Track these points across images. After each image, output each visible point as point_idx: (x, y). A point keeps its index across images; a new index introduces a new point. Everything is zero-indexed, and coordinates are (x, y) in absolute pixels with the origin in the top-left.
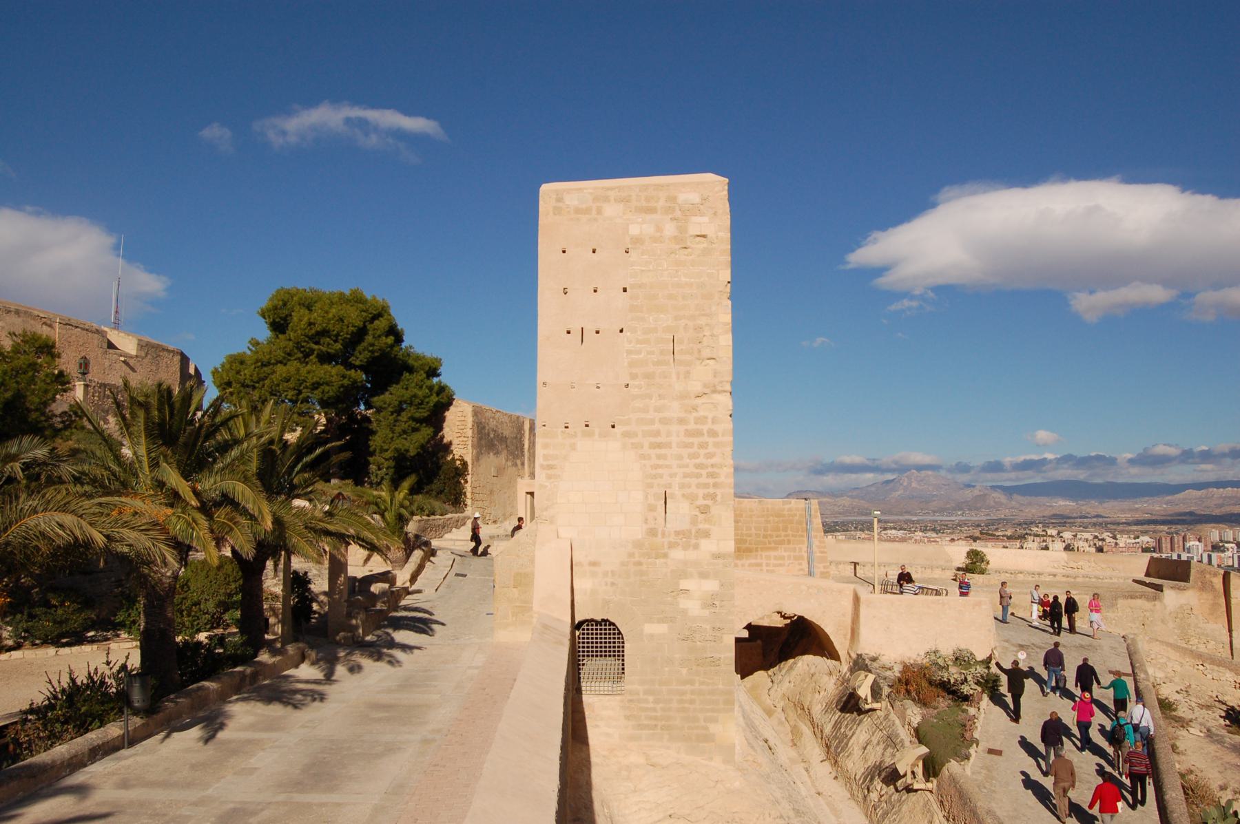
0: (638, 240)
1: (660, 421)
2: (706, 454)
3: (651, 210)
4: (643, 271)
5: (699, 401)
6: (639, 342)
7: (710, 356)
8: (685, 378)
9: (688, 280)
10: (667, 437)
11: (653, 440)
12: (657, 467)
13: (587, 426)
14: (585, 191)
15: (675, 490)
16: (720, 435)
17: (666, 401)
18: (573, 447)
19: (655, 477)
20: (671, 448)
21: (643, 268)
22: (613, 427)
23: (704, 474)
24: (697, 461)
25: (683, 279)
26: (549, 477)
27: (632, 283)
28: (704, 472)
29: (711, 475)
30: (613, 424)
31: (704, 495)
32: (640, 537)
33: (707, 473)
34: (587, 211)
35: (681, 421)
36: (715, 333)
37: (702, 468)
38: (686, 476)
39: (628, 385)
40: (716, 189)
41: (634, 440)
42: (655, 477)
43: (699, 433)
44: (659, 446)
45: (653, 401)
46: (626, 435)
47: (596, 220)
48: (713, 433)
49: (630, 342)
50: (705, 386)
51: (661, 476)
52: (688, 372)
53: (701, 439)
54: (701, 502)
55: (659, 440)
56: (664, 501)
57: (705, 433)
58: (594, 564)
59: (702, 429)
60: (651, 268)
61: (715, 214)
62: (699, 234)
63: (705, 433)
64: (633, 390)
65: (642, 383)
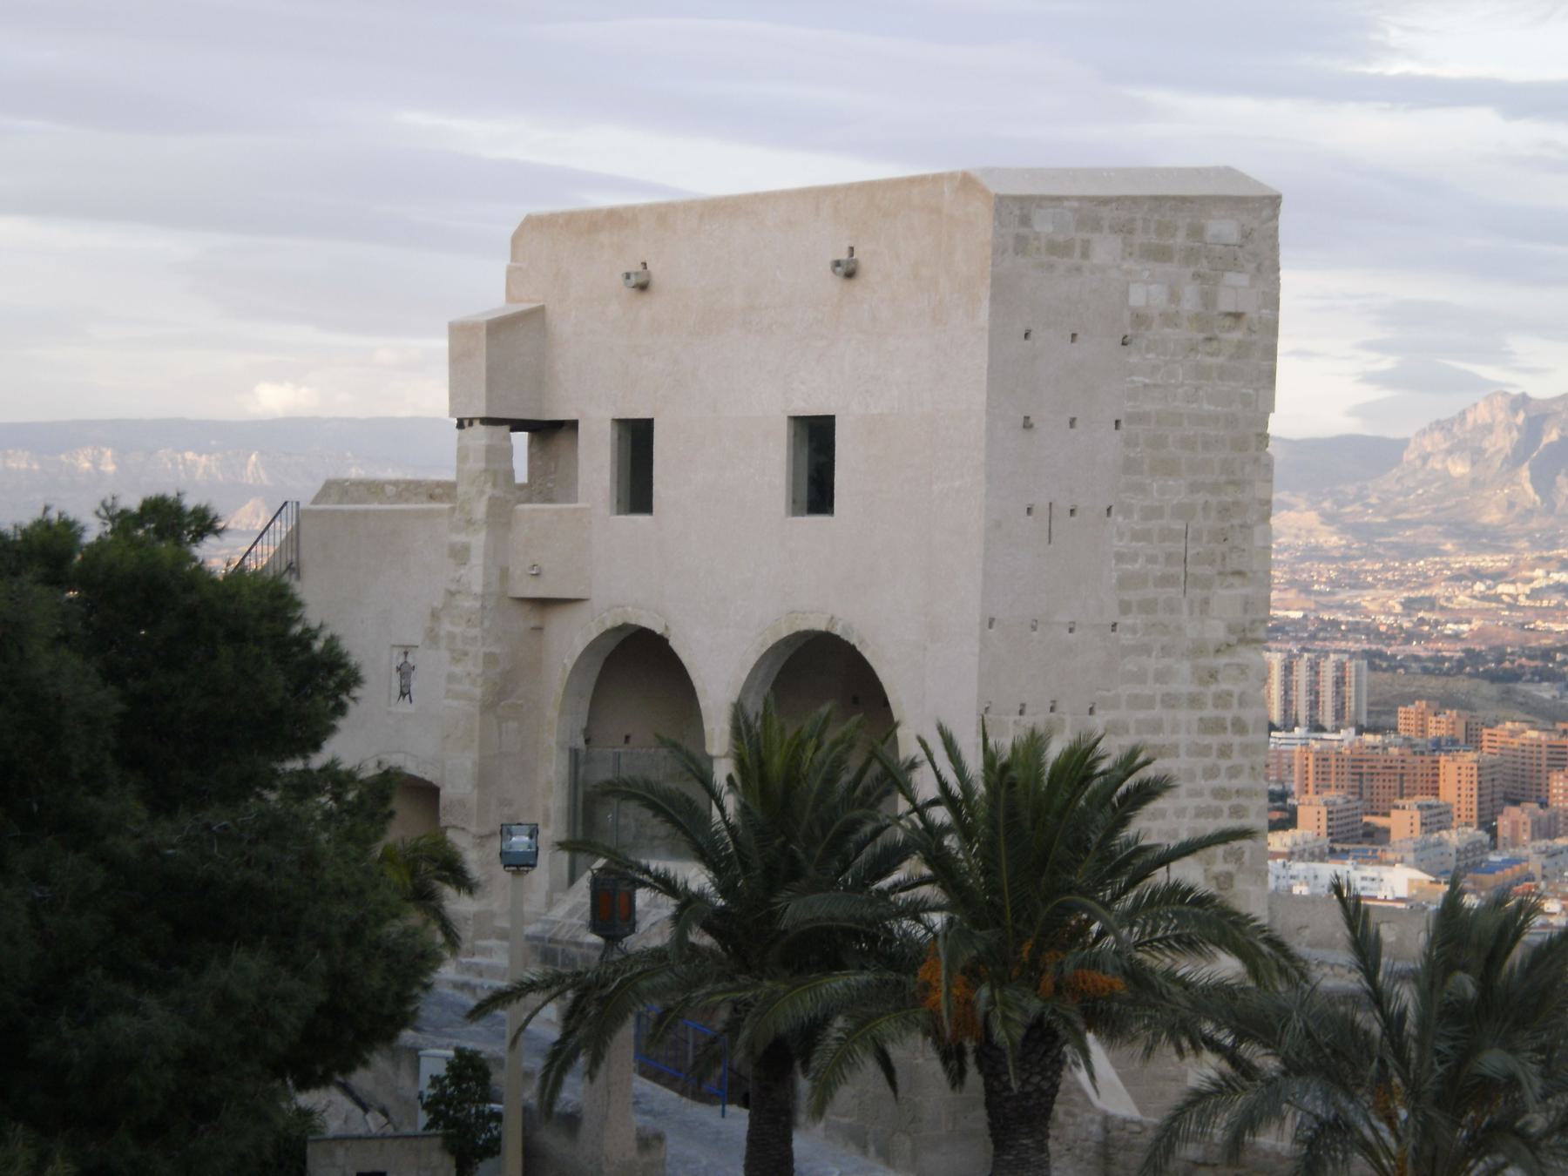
1: (1163, 701)
3: (1161, 254)
4: (1146, 386)
5: (1223, 660)
6: (1136, 536)
9: (1212, 408)
14: (1066, 204)
16: (1251, 730)
20: (1178, 756)
21: (1147, 381)
23: (1226, 812)
27: (1129, 410)
28: (1225, 805)
35: (1195, 701)
36: (1249, 521)
47: (1078, 269)
49: (1121, 536)
50: (1231, 629)
52: (1206, 601)
59: (1224, 719)
61: (1258, 269)
65: (1138, 621)
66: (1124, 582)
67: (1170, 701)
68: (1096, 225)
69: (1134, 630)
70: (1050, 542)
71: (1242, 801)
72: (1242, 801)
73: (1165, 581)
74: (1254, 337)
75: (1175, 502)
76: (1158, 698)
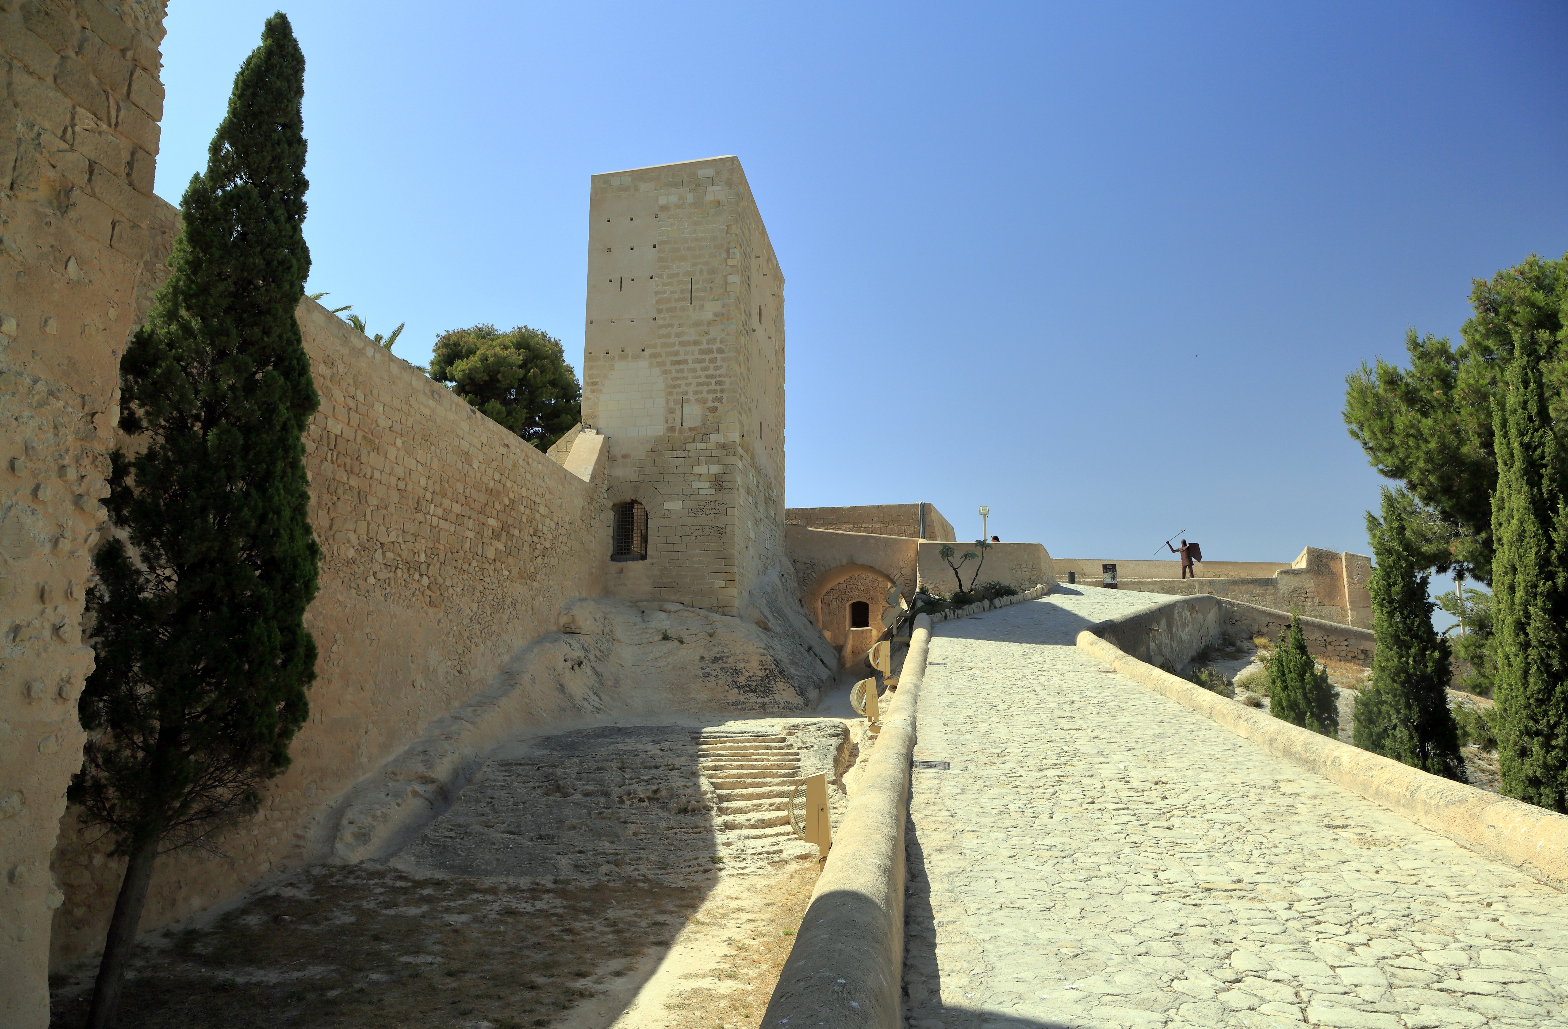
0: (664, 208)
6: (664, 285)
11: (673, 358)
12: (678, 378)
15: (691, 397)
19: (674, 387)
24: (708, 373)
26: (593, 391)
28: (713, 381)
29: (718, 383)
35: (696, 343)
38: (699, 384)
42: (674, 387)
43: (710, 351)
44: (679, 363)
46: (654, 356)
50: (716, 315)
51: (679, 386)
53: (711, 356)
54: (710, 404)
55: (678, 358)
58: (625, 456)
64: (660, 322)
69: (664, 319)
71: (722, 379)
72: (722, 379)
76: (677, 343)
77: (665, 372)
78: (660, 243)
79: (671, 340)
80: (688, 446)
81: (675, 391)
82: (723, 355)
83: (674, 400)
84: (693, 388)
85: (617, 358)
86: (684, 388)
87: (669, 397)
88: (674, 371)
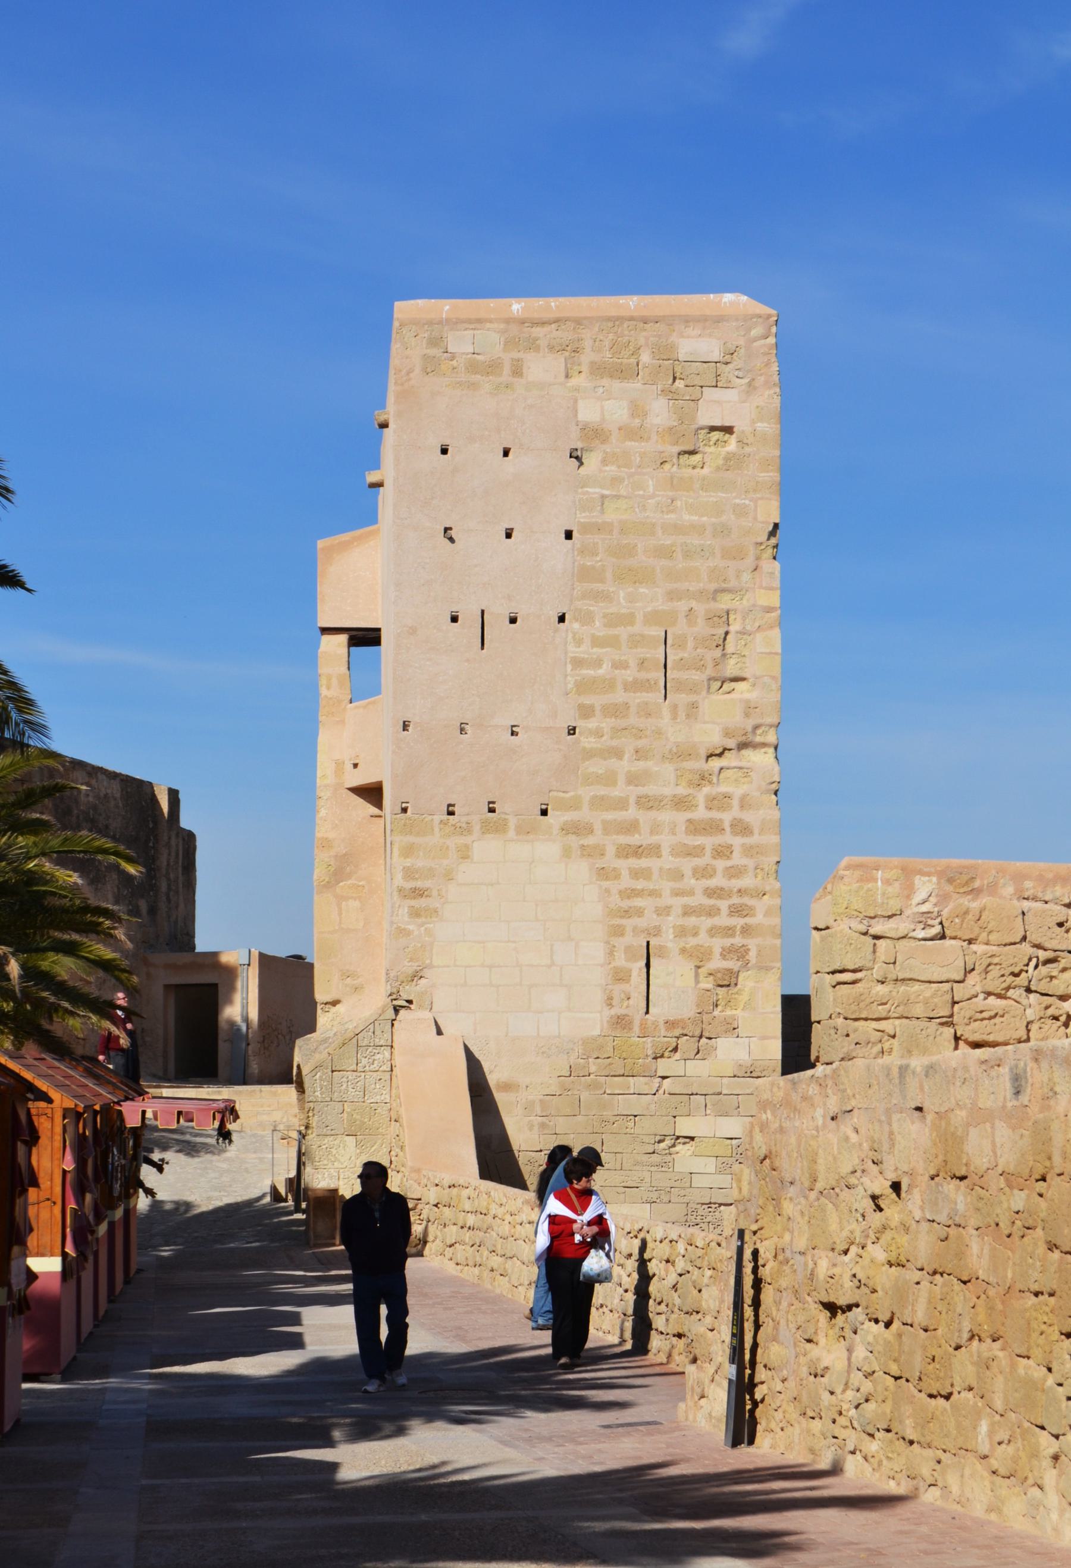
0: (595, 434)
1: (637, 803)
2: (727, 869)
4: (603, 497)
5: (716, 763)
6: (596, 642)
7: (736, 673)
8: (688, 716)
10: (652, 833)
11: (623, 839)
13: (492, 810)
14: (488, 325)
15: (667, 940)
16: (756, 831)
17: (650, 763)
18: (465, 854)
19: (627, 913)
21: (606, 492)
22: (544, 813)
23: (724, 911)
25: (687, 517)
26: (415, 913)
27: (582, 520)
28: (724, 905)
29: (736, 911)
30: (544, 807)
31: (723, 949)
32: (597, 1032)
33: (730, 907)
34: (492, 367)
35: (681, 803)
37: (720, 897)
38: (687, 911)
39: (574, 729)
40: (754, 333)
41: (590, 841)
42: (627, 913)
43: (714, 828)
44: (637, 851)
45: (625, 762)
46: (569, 829)
48: (741, 828)
49: (579, 642)
50: (727, 733)
51: (640, 912)
52: (694, 706)
54: (717, 963)
55: (635, 840)
56: (645, 961)
57: (727, 825)
59: (721, 820)
60: (623, 492)
62: (718, 423)
63: (728, 829)
65: (603, 725)
66: (584, 686)
67: (646, 803)
68: (532, 345)
69: (598, 733)
70: (483, 647)
71: (746, 900)
72: (746, 900)
73: (635, 686)
74: (747, 450)
75: (649, 609)
76: (632, 800)
77: (603, 873)
78: (586, 528)
79: (616, 792)
80: (663, 1066)
81: (628, 923)
82: (748, 840)
83: (628, 949)
84: (673, 920)
85: (477, 828)
86: (649, 919)
87: (615, 941)
88: (625, 873)
